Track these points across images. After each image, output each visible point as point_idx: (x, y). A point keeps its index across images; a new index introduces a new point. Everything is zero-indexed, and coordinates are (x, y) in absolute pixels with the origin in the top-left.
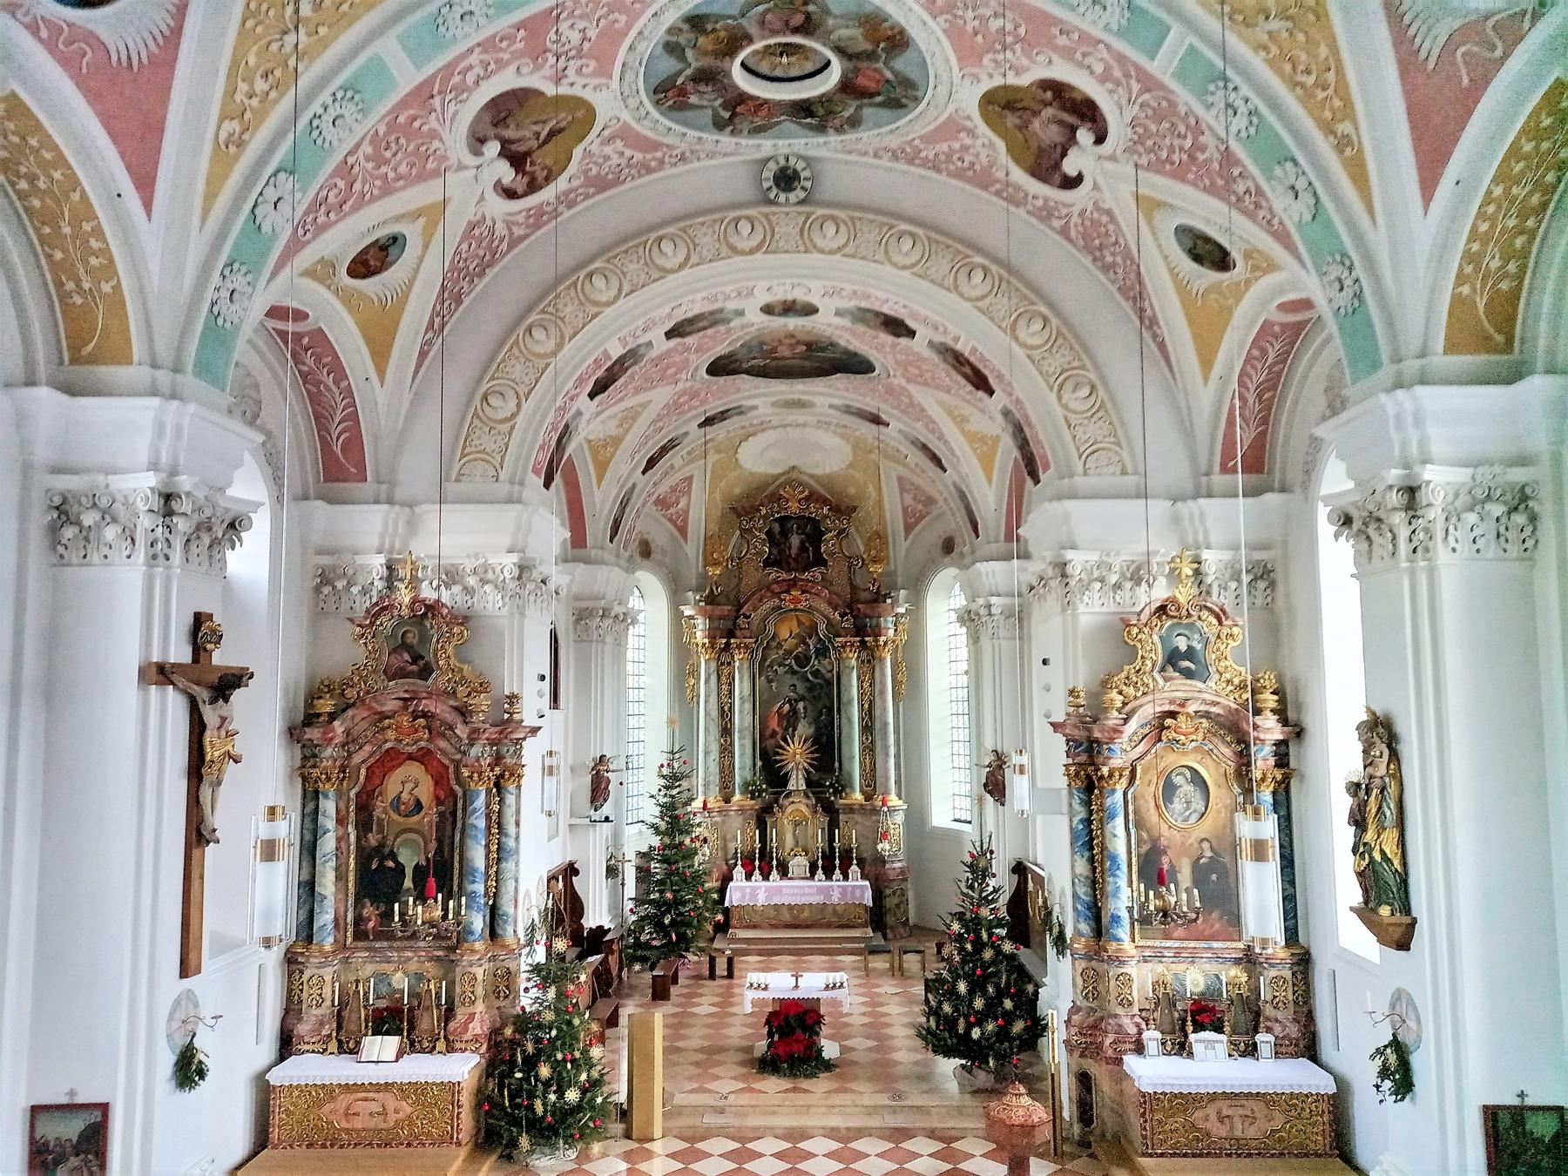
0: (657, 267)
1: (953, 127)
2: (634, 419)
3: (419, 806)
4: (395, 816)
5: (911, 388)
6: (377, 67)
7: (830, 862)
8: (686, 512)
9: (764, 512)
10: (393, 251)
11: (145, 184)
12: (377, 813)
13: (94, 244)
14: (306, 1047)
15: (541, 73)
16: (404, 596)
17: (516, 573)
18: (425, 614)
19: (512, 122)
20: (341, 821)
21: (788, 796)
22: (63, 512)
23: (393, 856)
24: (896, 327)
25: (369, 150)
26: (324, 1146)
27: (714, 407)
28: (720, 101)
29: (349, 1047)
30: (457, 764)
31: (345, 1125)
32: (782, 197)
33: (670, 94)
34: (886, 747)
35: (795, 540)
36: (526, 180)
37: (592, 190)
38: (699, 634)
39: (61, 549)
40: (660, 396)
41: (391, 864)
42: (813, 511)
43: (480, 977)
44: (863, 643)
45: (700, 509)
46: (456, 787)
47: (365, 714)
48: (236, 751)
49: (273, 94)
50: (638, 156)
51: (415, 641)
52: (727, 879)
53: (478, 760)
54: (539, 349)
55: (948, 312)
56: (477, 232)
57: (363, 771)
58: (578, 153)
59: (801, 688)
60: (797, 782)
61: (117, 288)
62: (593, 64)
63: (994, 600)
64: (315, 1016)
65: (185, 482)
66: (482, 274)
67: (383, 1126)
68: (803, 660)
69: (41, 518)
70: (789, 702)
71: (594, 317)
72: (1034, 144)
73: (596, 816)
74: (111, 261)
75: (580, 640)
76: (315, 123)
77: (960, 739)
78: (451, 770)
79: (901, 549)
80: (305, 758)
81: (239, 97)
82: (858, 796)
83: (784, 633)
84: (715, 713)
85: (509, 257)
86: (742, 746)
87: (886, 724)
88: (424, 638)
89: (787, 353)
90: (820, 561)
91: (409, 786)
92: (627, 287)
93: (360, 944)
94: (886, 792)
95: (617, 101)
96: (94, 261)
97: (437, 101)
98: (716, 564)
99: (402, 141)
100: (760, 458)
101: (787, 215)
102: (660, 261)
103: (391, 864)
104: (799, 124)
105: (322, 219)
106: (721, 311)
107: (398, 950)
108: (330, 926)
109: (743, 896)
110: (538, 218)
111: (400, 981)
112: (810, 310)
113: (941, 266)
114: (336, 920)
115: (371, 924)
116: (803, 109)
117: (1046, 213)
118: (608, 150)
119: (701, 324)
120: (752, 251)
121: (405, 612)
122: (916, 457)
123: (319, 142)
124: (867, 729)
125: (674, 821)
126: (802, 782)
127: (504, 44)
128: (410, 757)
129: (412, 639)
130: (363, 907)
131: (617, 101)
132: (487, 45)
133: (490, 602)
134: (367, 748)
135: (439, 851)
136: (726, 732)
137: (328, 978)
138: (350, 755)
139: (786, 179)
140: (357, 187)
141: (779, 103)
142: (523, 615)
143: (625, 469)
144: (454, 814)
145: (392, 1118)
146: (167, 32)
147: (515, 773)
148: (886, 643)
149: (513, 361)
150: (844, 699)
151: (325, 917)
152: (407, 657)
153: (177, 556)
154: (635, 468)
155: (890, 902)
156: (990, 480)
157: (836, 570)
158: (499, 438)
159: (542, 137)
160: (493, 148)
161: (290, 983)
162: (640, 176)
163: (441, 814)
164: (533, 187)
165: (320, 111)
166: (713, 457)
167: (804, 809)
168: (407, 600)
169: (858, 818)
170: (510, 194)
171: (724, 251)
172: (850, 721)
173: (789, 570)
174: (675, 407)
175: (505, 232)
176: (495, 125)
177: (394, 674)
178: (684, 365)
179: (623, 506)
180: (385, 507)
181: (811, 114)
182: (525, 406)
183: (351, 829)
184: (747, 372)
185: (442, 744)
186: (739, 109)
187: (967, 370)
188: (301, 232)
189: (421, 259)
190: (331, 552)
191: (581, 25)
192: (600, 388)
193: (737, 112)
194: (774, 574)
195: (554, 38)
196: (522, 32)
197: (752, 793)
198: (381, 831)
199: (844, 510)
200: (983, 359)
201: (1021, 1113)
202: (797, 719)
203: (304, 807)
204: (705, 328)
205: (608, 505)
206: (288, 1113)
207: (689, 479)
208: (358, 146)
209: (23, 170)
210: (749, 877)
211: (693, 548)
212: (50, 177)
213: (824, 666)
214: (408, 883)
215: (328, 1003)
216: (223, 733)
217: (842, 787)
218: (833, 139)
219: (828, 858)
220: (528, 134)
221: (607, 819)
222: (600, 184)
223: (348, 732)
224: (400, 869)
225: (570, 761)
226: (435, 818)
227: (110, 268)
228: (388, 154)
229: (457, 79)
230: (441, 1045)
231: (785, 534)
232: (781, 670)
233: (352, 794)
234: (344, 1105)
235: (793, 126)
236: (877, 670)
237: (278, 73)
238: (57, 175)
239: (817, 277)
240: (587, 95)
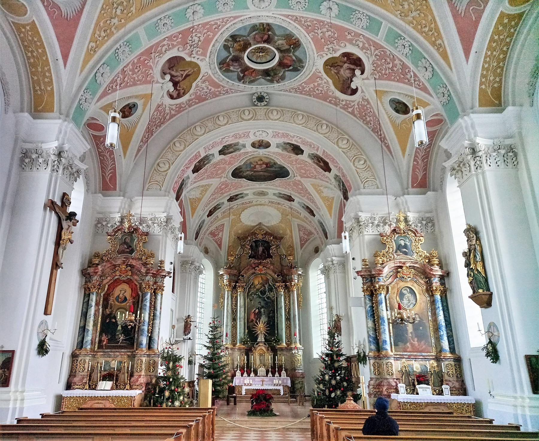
0: (218, 124)
1: (315, 77)
2: (206, 191)
4: (117, 303)
5: (303, 180)
6: (137, 37)
7: (274, 369)
8: (221, 239)
9: (249, 239)
10: (133, 110)
11: (65, 57)
12: (111, 302)
13: (47, 74)
14: (77, 387)
15: (184, 52)
16: (126, 225)
17: (165, 220)
18: (133, 232)
19: (174, 69)
20: (97, 304)
21: (257, 344)
22: (25, 154)
23: (115, 318)
24: (297, 150)
25: (131, 67)
27: (233, 193)
28: (240, 69)
29: (93, 387)
30: (141, 284)
32: (259, 104)
33: (225, 65)
34: (295, 325)
35: (261, 249)
36: (177, 92)
37: (197, 101)
38: (225, 281)
39: (23, 166)
40: (215, 182)
41: (114, 320)
42: (267, 238)
43: (144, 361)
44: (286, 285)
45: (226, 238)
46: (140, 293)
47: (109, 265)
48: (72, 239)
49: (106, 38)
50: (213, 89)
52: (234, 375)
53: (148, 281)
54: (178, 149)
55: (315, 140)
56: (160, 109)
57: (107, 286)
58: (194, 85)
59: (263, 303)
60: (261, 338)
61: (52, 89)
62: (201, 50)
63: (334, 258)
64: (82, 374)
65: (66, 147)
66: (160, 126)
68: (263, 293)
69: (18, 155)
70: (258, 308)
71: (196, 139)
72: (341, 79)
73: (186, 337)
74: (52, 80)
75: (182, 272)
76: (117, 51)
77: (323, 307)
78: (138, 286)
79: (299, 252)
80: (86, 282)
81: (96, 35)
82: (284, 344)
83: (256, 282)
84: (230, 311)
85: (169, 121)
86: (240, 324)
87: (294, 316)
88: (132, 240)
89: (259, 169)
90: (271, 257)
91: (123, 292)
92: (207, 130)
94: (296, 342)
95: (208, 66)
96: (46, 80)
97: (153, 55)
98: (232, 256)
99: (141, 67)
100: (249, 219)
101: (261, 109)
102: (218, 122)
103: (114, 320)
104: (265, 79)
105: (114, 87)
106: (237, 144)
108: (90, 342)
109: (240, 382)
110: (180, 109)
111: (114, 364)
112: (267, 145)
113: (312, 124)
114: (92, 341)
115: (105, 343)
116: (266, 73)
117: (345, 107)
118: (204, 85)
119: (231, 150)
120: (249, 120)
121: (126, 230)
122: (305, 214)
123: (117, 58)
124: (288, 319)
125: (214, 342)
126: (263, 338)
127: (175, 39)
129: (128, 240)
131: (208, 66)
132: (170, 38)
133: (156, 230)
134: (109, 278)
136: (234, 319)
137: (87, 361)
139: (261, 99)
140: (126, 79)
141: (259, 70)
142: (167, 236)
143: (201, 213)
144: (138, 302)
146: (79, 10)
147: (161, 288)
148: (294, 285)
149: (168, 153)
150: (279, 307)
151: (89, 338)
152: (126, 246)
153: (60, 171)
154: (204, 214)
155: (298, 386)
156: (331, 216)
157: (276, 259)
158: (162, 177)
159: (184, 76)
160: (168, 77)
161: (73, 365)
162: (213, 98)
163: (133, 302)
164: (179, 96)
165: (119, 47)
166: (232, 217)
167: (263, 348)
168: (127, 226)
169: (285, 353)
170: (172, 97)
171: (240, 120)
172: (281, 315)
173: (258, 259)
174: (220, 190)
175: (168, 111)
176: (169, 69)
177: (120, 252)
178: (225, 169)
179: (200, 227)
180: (122, 198)
181: (269, 76)
182: (171, 167)
184: (245, 177)
185: (136, 277)
186: (246, 73)
187: (322, 164)
188: (107, 89)
189: (142, 114)
190: (102, 213)
191: (199, 35)
192: (196, 170)
193: (246, 75)
194: (253, 260)
195: (190, 39)
196: (180, 36)
197: (244, 342)
199: (279, 238)
200: (328, 155)
201: (351, 405)
202: (261, 316)
203: (84, 300)
204: (232, 152)
205: (194, 226)
207: (223, 225)
208: (128, 65)
209: (30, 49)
210: (242, 375)
211: (223, 253)
212: (38, 51)
213: (271, 295)
214: (119, 328)
215: (86, 370)
216: (68, 232)
217: (278, 340)
218: (276, 85)
219: (273, 368)
220: (178, 74)
221: (190, 338)
222: (200, 99)
223: (103, 271)
225: (177, 317)
226: (131, 304)
227: (51, 83)
228: (136, 70)
229: (160, 48)
230: (128, 387)
231: (257, 246)
232: (255, 296)
233: (102, 295)
235: (262, 80)
236: (291, 295)
237: (108, 31)
238: (40, 51)
239: (271, 128)
240: (199, 62)
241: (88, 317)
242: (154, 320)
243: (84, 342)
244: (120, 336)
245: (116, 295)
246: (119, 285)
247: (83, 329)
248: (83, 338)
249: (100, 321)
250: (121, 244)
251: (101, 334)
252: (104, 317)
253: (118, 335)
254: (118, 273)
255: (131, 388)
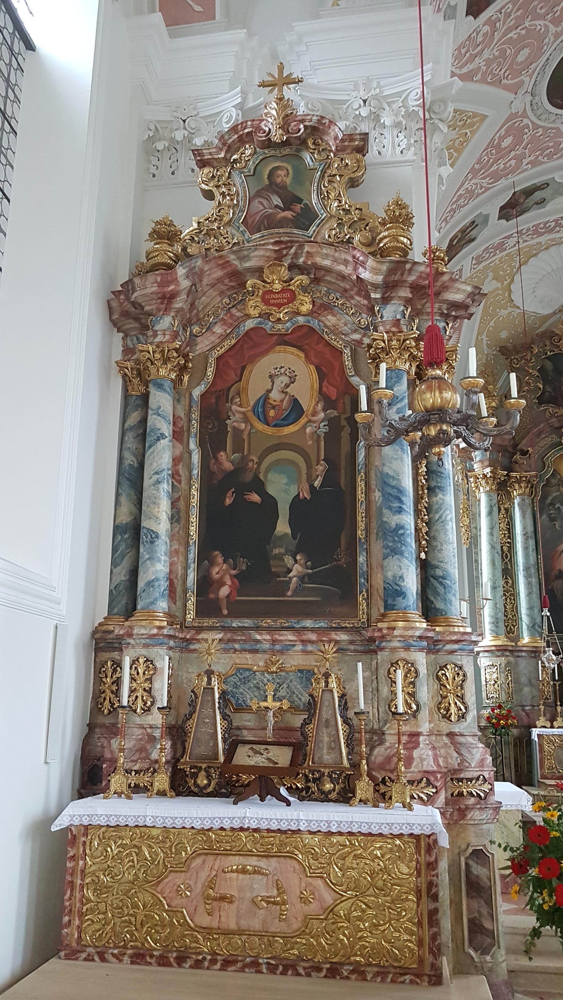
3: (296, 410)
4: (260, 426)
12: (235, 421)
20: (179, 435)
23: (258, 486)
26: (163, 961)
27: (524, 179)
31: (205, 920)
41: (255, 498)
43: (423, 670)
47: (219, 273)
51: (288, 181)
57: (212, 360)
67: (276, 926)
88: (302, 174)
93: (208, 622)
103: (255, 498)
107: (269, 630)
108: (164, 585)
115: (224, 591)
128: (283, 340)
130: (212, 563)
134: (218, 329)
135: (330, 477)
138: (192, 340)
145: (296, 910)
151: (157, 567)
152: (276, 201)
161: (99, 680)
163: (332, 423)
183: (193, 445)
198: (238, 447)
206: (100, 888)
214: (283, 527)
224: (270, 503)
226: (323, 429)
233: (197, 392)
234: (203, 875)
241: (147, 482)
242: (431, 490)
243: (141, 584)
244: (288, 560)
245: (254, 393)
246: (266, 352)
247: (131, 536)
248: (134, 573)
249: (195, 501)
250: (258, 194)
251: (204, 556)
252: (214, 486)
253: (280, 557)
254: (254, 306)
255: (382, 797)
